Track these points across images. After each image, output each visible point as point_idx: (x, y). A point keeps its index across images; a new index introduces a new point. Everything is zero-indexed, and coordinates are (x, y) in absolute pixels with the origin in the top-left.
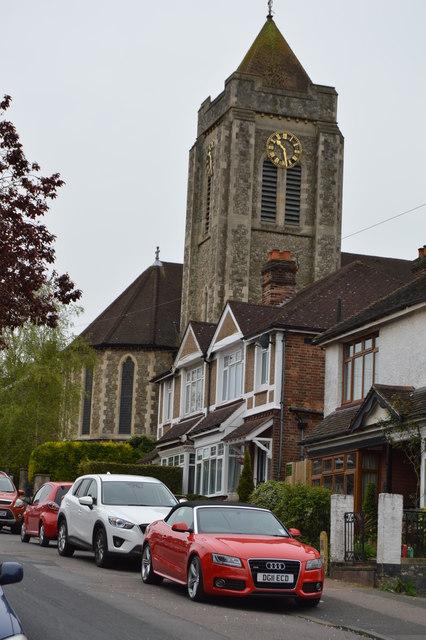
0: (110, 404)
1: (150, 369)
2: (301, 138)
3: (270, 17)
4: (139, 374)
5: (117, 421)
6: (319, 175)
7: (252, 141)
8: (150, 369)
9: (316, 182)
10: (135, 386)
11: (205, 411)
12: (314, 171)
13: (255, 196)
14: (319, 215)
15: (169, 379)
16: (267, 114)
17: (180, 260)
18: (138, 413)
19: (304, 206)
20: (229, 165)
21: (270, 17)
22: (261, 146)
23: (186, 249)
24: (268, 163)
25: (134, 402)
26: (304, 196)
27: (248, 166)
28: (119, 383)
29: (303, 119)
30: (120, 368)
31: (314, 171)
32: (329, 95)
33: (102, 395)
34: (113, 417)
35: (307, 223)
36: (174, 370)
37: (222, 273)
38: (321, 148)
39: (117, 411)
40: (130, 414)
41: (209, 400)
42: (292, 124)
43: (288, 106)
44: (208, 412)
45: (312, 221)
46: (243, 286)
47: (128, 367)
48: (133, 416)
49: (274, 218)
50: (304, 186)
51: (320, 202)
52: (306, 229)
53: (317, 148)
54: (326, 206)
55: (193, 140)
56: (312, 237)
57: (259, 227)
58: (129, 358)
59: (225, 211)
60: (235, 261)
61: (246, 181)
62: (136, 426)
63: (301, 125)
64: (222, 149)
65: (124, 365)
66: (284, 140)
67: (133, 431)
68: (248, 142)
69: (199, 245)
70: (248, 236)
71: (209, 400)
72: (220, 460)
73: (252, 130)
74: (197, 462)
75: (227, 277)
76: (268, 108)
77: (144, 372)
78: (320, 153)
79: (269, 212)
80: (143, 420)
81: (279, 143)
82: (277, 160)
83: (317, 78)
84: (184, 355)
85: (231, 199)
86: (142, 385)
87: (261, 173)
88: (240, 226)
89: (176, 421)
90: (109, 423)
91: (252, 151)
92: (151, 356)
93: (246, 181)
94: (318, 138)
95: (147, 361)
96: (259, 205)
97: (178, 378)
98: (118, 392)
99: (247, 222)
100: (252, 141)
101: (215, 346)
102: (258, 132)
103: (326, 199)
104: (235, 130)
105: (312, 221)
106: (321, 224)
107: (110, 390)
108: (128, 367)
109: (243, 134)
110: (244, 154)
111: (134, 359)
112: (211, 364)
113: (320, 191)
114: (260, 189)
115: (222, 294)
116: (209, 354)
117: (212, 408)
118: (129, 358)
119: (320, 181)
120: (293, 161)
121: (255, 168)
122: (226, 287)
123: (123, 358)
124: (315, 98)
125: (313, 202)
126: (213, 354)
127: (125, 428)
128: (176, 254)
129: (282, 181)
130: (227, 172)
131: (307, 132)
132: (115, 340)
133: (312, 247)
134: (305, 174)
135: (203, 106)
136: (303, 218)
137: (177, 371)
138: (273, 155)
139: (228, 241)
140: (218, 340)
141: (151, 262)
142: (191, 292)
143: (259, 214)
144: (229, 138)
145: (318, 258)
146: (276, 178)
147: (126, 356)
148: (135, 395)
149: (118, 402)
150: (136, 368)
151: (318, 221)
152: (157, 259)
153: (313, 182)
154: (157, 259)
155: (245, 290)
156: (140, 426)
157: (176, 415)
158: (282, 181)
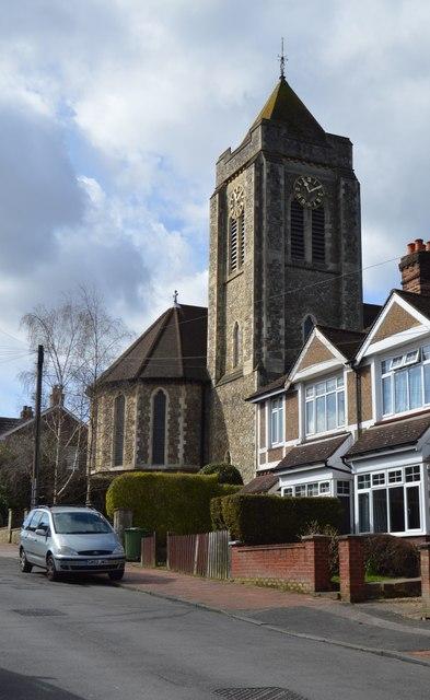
0: (142, 435)
1: (182, 401)
2: (323, 182)
3: (283, 78)
5: (150, 451)
6: (342, 217)
7: (282, 182)
8: (182, 401)
9: (339, 222)
10: (167, 417)
11: (353, 428)
12: (336, 212)
13: (286, 235)
14: (344, 253)
15: (279, 397)
16: (293, 158)
17: (204, 304)
18: (171, 444)
19: (328, 245)
20: (261, 204)
21: (283, 78)
22: (289, 188)
23: (211, 289)
24: (297, 208)
25: (167, 434)
26: (328, 235)
27: (279, 204)
28: (151, 415)
29: (324, 165)
30: (151, 401)
31: (336, 212)
32: (344, 145)
33: (134, 427)
34: (147, 448)
35: (332, 261)
36: (287, 385)
37: (258, 307)
38: (343, 191)
39: (150, 442)
40: (163, 445)
41: (359, 413)
42: (315, 169)
43: (311, 153)
44: (359, 430)
45: (336, 259)
46: (280, 317)
47: (160, 398)
48: (166, 447)
49: (303, 255)
50: (328, 226)
51: (344, 241)
52: (331, 266)
53: (338, 192)
54: (349, 245)
55: (211, 187)
56: (337, 273)
57: (290, 261)
58: (161, 392)
59: (258, 247)
60: (271, 294)
61: (278, 219)
63: (322, 170)
65: (156, 398)
66: (311, 185)
67: (166, 460)
68: (278, 182)
70: (282, 271)
71: (359, 413)
72: (414, 492)
73: (281, 171)
74: (358, 492)
75: (264, 309)
76: (293, 153)
77: (175, 405)
78: (341, 196)
79: (297, 249)
80: (176, 451)
81: (306, 184)
82: (303, 201)
83: (328, 129)
84: (306, 365)
85: (264, 235)
86: (174, 416)
87: (289, 213)
88: (274, 261)
89: (294, 443)
90: (142, 454)
91: (282, 191)
92: (183, 389)
93: (278, 219)
94: (338, 183)
95: (179, 394)
96: (289, 242)
97: (291, 393)
98: (151, 424)
99: (280, 257)
100: (282, 182)
101: (369, 349)
102: (286, 174)
103: (349, 238)
104: (265, 171)
105: (336, 259)
106: (346, 261)
107: (142, 422)
108: (160, 398)
109: (273, 174)
110: (274, 194)
111: (166, 392)
112: (361, 370)
113: (344, 231)
114: (289, 227)
116: (359, 358)
117: (367, 425)
119: (343, 221)
120: (317, 202)
121: (286, 209)
122: (264, 319)
123: (154, 393)
124: (333, 145)
125: (336, 241)
126: (364, 359)
127: (158, 459)
128: (196, 291)
129: (308, 220)
130: (258, 211)
131: (329, 177)
132: (146, 374)
133: (338, 283)
134: (328, 216)
135: (222, 158)
136: (328, 256)
137: (293, 386)
138: (299, 196)
139: (264, 274)
140: (375, 340)
141: (171, 305)
142: (218, 329)
143: (289, 249)
144: (259, 180)
145: (345, 293)
146: (302, 218)
147: (157, 389)
148: (167, 426)
149: (151, 434)
150: (168, 401)
151: (343, 258)
152: (175, 301)
153: (336, 222)
154: (175, 301)
155: (282, 322)
156: (174, 456)
157: (291, 436)
158: (308, 220)
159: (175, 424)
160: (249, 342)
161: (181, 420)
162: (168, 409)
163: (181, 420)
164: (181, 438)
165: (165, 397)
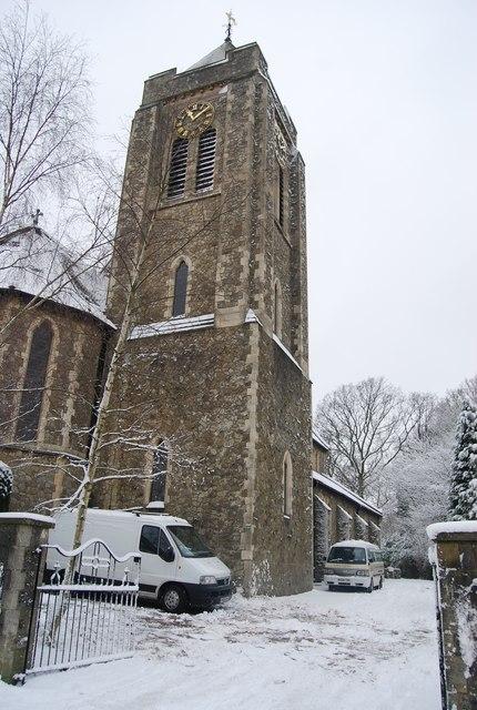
1: (78, 348)
3: (228, 40)
4: (59, 349)
10: (52, 367)
21: (228, 40)
28: (25, 355)
30: (30, 334)
58: (46, 325)
62: (46, 428)
64: (249, 104)
65: (37, 332)
67: (41, 437)
69: (151, 212)
111: (55, 328)
115: (254, 266)
118: (46, 325)
150: (56, 342)
156: (54, 432)
159: (62, 379)
160: (231, 281)
161: (72, 375)
162: (55, 354)
163: (72, 375)
164: (70, 403)
165: (52, 334)
